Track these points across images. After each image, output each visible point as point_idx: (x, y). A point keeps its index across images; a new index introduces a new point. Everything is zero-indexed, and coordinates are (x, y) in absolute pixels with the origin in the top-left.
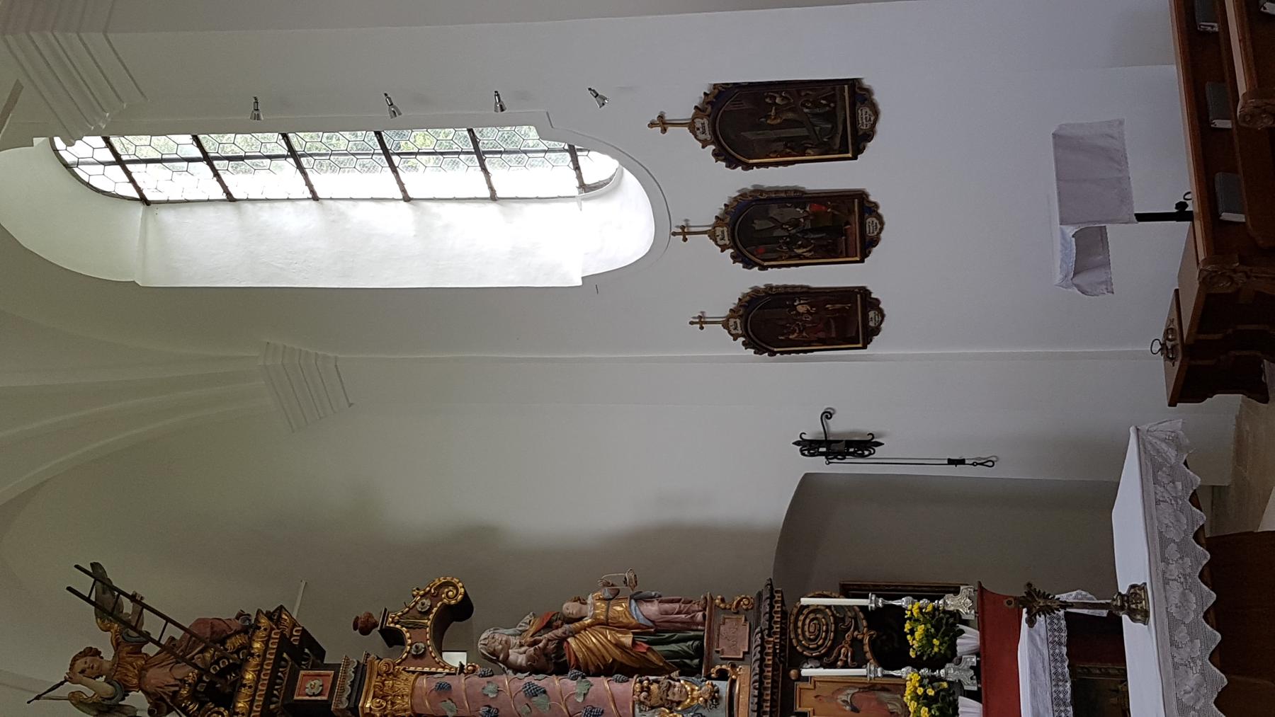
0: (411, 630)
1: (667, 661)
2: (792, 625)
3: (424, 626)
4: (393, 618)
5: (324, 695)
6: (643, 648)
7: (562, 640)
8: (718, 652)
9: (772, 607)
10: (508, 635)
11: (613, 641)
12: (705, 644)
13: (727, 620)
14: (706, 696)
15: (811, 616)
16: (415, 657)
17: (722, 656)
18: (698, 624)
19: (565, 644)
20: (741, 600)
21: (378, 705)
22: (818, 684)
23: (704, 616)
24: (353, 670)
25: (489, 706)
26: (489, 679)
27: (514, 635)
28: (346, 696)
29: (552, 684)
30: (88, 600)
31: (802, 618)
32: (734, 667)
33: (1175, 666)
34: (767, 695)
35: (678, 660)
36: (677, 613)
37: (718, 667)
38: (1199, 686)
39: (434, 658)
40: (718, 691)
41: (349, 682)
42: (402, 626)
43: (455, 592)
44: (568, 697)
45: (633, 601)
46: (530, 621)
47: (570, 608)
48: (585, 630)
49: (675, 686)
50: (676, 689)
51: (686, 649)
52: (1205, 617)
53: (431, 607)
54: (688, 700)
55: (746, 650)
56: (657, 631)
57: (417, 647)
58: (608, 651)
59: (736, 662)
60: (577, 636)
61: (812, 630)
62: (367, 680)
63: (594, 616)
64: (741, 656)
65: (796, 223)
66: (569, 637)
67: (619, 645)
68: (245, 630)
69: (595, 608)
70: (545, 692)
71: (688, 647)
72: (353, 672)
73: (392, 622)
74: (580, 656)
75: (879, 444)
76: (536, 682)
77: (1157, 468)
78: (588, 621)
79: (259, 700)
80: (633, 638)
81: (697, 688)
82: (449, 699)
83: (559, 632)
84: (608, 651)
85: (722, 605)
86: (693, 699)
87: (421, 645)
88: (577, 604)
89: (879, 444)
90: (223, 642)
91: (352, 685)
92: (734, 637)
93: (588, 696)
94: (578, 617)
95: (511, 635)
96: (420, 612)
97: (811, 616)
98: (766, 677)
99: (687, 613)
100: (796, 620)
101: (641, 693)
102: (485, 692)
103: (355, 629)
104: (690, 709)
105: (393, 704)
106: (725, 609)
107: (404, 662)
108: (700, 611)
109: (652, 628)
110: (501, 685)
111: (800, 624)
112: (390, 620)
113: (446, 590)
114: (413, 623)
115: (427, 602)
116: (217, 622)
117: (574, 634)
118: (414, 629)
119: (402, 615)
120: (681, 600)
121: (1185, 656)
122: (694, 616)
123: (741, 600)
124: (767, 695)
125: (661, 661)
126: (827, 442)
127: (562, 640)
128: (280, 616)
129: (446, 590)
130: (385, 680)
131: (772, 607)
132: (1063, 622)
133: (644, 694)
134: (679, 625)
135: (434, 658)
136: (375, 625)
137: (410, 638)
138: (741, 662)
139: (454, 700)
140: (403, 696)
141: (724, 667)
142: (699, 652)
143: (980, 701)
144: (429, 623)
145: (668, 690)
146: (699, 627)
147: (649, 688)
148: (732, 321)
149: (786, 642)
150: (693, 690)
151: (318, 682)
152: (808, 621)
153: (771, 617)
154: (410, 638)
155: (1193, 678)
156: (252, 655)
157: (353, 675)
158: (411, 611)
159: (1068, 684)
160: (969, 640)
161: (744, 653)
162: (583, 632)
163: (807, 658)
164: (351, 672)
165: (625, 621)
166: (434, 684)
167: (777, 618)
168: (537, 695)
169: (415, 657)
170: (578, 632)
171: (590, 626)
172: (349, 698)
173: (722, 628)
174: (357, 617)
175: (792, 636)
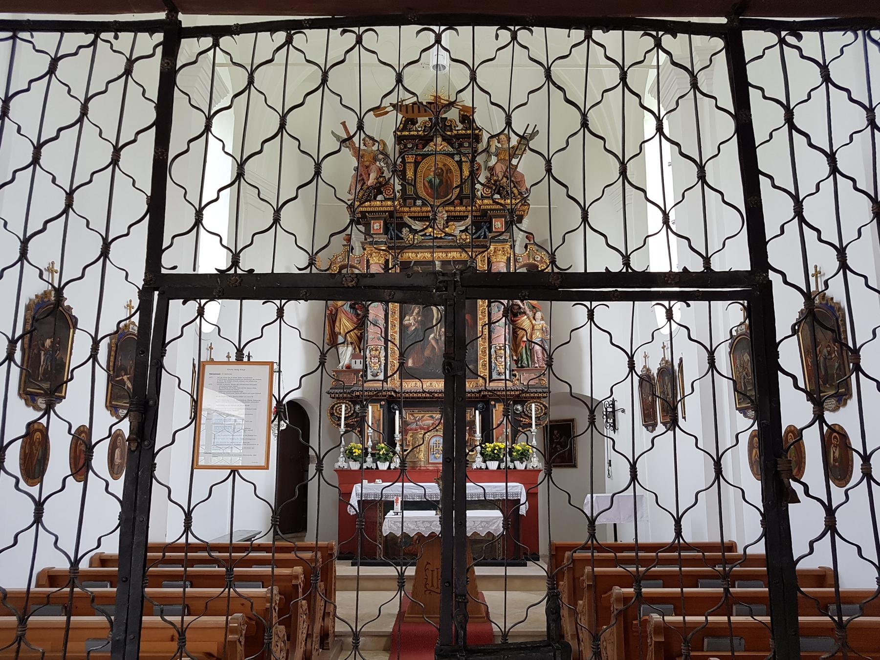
3: (529, 260)
6: (523, 345)
7: (525, 313)
9: (540, 393)
15: (539, 408)
30: (525, 133)
32: (518, 380)
33: (416, 522)
36: (537, 357)
38: (410, 528)
47: (539, 315)
52: (433, 532)
56: (530, 350)
63: (536, 325)
65: (668, 395)
67: (522, 337)
68: (520, 193)
74: (519, 321)
75: (615, 432)
77: (487, 522)
78: (534, 322)
79: (489, 207)
83: (528, 312)
87: (521, 260)
88: (540, 318)
89: (615, 432)
90: (515, 186)
97: (539, 408)
99: (538, 361)
100: (538, 402)
115: (539, 259)
116: (523, 182)
117: (528, 318)
121: (420, 525)
126: (614, 412)
127: (525, 313)
128: (525, 205)
131: (540, 393)
132: (516, 498)
142: (522, 367)
143: (498, 469)
148: (645, 369)
151: (500, 226)
153: (536, 393)
155: (412, 527)
156: (505, 200)
159: (492, 499)
160: (520, 466)
163: (523, 407)
165: (533, 337)
167: (536, 395)
170: (529, 319)
171: (532, 323)
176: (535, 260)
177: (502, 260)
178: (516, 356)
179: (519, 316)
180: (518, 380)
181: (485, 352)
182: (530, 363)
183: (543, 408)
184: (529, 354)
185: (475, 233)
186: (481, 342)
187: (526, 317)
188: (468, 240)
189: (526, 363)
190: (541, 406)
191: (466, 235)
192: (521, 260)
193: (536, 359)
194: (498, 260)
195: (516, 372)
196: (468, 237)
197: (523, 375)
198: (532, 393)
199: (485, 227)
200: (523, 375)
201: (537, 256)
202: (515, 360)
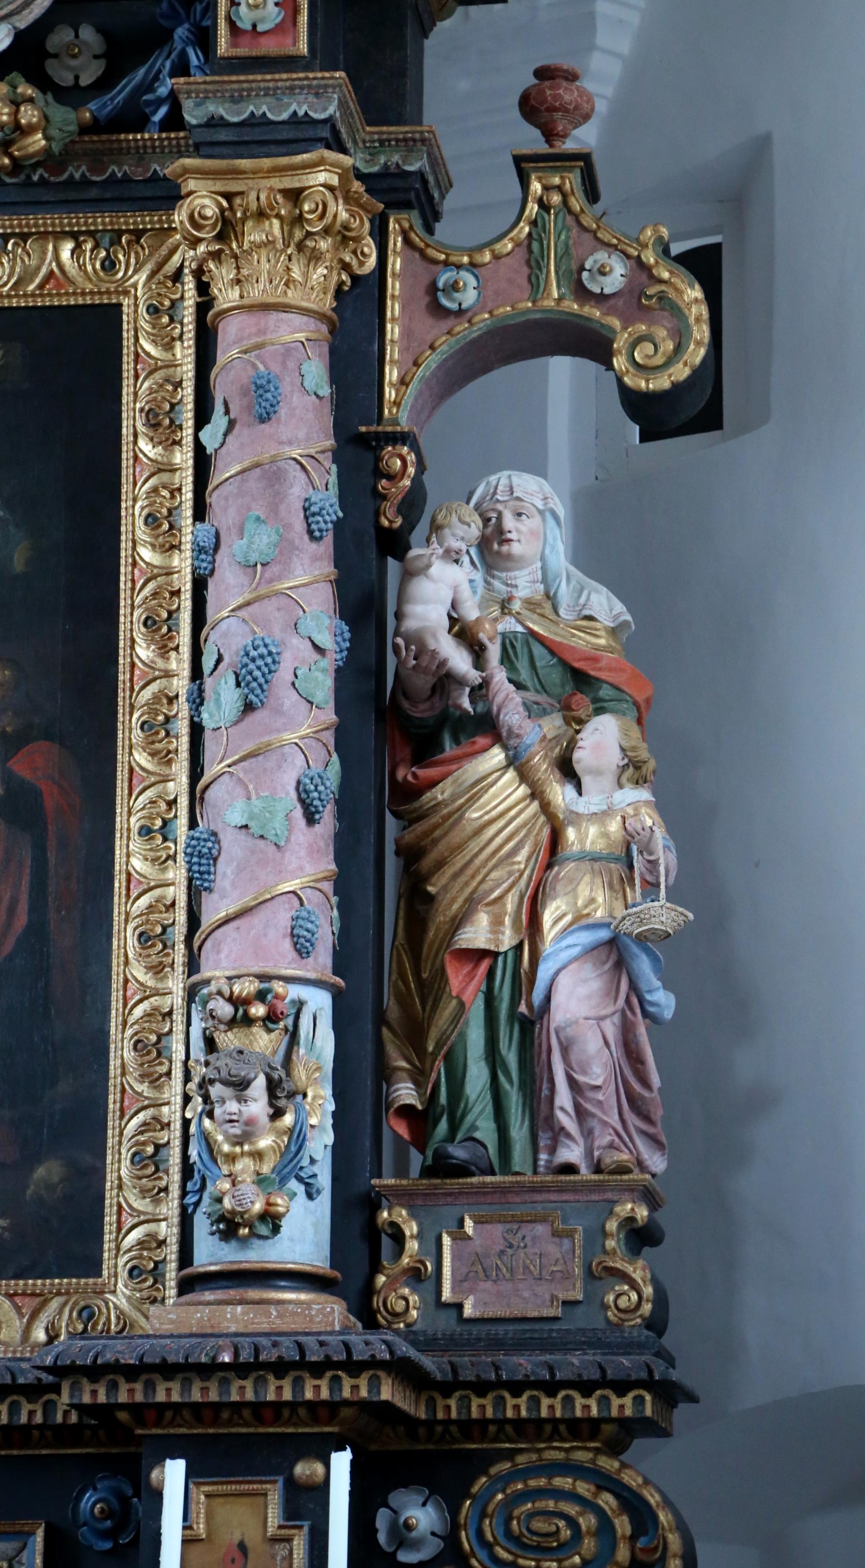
0: (522, 253)
1: (440, 1066)
2: (560, 1456)
3: (535, 285)
4: (559, 188)
5: (234, 44)
8: (461, 1223)
10: (543, 558)
11: (485, 886)
12: (474, 1180)
13: (566, 1242)
14: (227, 1203)
16: (433, 289)
17: (446, 1240)
18: (552, 1150)
19: (481, 741)
20: (634, 1286)
21: (196, 215)
22: (281, 1550)
23: (569, 1169)
24: (301, 113)
25: (217, 547)
26: (299, 525)
27: (545, 580)
28: (222, 111)
29: (280, 722)
31: (583, 1488)
32: (415, 1275)
34: (205, 1390)
35: (443, 1099)
36: (574, 1085)
37: (411, 1228)
39: (432, 347)
40: (253, 1234)
41: (264, 108)
42: (534, 223)
43: (659, 360)
44: (240, 780)
45: (604, 934)
46: (590, 618)
48: (533, 796)
49: (241, 1100)
50: (232, 1106)
51: (469, 1118)
53: (601, 298)
54: (226, 1148)
55: (468, 1311)
57: (454, 287)
58: (456, 876)
59: (429, 1285)
60: (511, 774)
61: (539, 1525)
62: (267, 163)
63: (575, 818)
64: (447, 1294)
66: (505, 748)
69: (601, 817)
70: (248, 708)
71: (474, 1127)
72: (295, 113)
73: (546, 188)
74: (440, 793)
76: (284, 674)
80: (495, 955)
81: (266, 1169)
82: (232, 424)
84: (456, 876)
85: (612, 1225)
86: (231, 1158)
87: (469, 297)
88: (615, 758)
91: (252, 122)
92: (511, 1270)
93: (242, 835)
94: (578, 768)
95: (544, 569)
96: (582, 268)
97: (588, 1521)
98: (260, 1383)
99: (581, 1113)
101: (231, 1000)
102: (250, 526)
103: (542, 74)
104: (205, 1157)
105: (216, 256)
106: (605, 1234)
107: (417, 255)
108: (589, 1152)
109: (530, 1005)
110: (275, 569)
111: (563, 1482)
112: (557, 181)
113: (661, 333)
114: (544, 252)
118: (528, 263)
119: (570, 211)
120: (645, 1083)
122: (569, 1136)
123: (634, 1286)
124: (205, 1390)
125: (439, 1045)
129: (661, 333)
130: (278, 216)
131: (586, 1388)
133: (225, 1010)
134: (545, 1092)
135: (432, 347)
136: (550, 135)
137: (496, 257)
138: (431, 1299)
139: (230, 438)
140: (238, 282)
141: (413, 1246)
144: (549, 303)
145: (226, 1083)
146: (543, 1157)
147: (248, 1021)
149: (496, 1440)
150: (258, 1155)
152: (572, 1509)
153: (551, 1388)
154: (496, 257)
157: (285, 116)
158: (587, 237)
161: (459, 1307)
162: (523, 790)
163: (454, 1511)
164: (294, 107)
165: (547, 918)
166: (275, 368)
168: (238, 685)
169: (433, 289)
170: (524, 776)
171: (546, 807)
172: (214, 123)
173: (541, 1229)
174: (572, 77)
175: (521, 1459)
176: (582, 293)
177: (293, 296)
178: (419, 1077)
179: (449, 749)
180: (415, 1275)
181: (160, 1050)
182: (519, 1132)
183: (623, 1525)
184: (511, 1058)
185: (103, 85)
186: (139, 972)
187: (496, 756)
188: (37, 141)
189: (486, 1131)
190: (607, 1501)
191: (16, 103)
192: (469, 297)
193: (563, 1097)
194: (256, 293)
195: (401, 1214)
196: (28, 115)
197: (459, 1236)
198: (516, 1388)
199: (181, 32)
200: (459, 1236)
201: (601, 256)
202: (406, 1111)
